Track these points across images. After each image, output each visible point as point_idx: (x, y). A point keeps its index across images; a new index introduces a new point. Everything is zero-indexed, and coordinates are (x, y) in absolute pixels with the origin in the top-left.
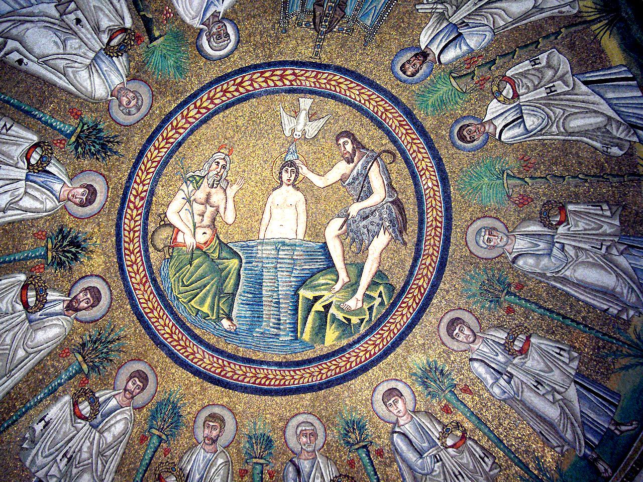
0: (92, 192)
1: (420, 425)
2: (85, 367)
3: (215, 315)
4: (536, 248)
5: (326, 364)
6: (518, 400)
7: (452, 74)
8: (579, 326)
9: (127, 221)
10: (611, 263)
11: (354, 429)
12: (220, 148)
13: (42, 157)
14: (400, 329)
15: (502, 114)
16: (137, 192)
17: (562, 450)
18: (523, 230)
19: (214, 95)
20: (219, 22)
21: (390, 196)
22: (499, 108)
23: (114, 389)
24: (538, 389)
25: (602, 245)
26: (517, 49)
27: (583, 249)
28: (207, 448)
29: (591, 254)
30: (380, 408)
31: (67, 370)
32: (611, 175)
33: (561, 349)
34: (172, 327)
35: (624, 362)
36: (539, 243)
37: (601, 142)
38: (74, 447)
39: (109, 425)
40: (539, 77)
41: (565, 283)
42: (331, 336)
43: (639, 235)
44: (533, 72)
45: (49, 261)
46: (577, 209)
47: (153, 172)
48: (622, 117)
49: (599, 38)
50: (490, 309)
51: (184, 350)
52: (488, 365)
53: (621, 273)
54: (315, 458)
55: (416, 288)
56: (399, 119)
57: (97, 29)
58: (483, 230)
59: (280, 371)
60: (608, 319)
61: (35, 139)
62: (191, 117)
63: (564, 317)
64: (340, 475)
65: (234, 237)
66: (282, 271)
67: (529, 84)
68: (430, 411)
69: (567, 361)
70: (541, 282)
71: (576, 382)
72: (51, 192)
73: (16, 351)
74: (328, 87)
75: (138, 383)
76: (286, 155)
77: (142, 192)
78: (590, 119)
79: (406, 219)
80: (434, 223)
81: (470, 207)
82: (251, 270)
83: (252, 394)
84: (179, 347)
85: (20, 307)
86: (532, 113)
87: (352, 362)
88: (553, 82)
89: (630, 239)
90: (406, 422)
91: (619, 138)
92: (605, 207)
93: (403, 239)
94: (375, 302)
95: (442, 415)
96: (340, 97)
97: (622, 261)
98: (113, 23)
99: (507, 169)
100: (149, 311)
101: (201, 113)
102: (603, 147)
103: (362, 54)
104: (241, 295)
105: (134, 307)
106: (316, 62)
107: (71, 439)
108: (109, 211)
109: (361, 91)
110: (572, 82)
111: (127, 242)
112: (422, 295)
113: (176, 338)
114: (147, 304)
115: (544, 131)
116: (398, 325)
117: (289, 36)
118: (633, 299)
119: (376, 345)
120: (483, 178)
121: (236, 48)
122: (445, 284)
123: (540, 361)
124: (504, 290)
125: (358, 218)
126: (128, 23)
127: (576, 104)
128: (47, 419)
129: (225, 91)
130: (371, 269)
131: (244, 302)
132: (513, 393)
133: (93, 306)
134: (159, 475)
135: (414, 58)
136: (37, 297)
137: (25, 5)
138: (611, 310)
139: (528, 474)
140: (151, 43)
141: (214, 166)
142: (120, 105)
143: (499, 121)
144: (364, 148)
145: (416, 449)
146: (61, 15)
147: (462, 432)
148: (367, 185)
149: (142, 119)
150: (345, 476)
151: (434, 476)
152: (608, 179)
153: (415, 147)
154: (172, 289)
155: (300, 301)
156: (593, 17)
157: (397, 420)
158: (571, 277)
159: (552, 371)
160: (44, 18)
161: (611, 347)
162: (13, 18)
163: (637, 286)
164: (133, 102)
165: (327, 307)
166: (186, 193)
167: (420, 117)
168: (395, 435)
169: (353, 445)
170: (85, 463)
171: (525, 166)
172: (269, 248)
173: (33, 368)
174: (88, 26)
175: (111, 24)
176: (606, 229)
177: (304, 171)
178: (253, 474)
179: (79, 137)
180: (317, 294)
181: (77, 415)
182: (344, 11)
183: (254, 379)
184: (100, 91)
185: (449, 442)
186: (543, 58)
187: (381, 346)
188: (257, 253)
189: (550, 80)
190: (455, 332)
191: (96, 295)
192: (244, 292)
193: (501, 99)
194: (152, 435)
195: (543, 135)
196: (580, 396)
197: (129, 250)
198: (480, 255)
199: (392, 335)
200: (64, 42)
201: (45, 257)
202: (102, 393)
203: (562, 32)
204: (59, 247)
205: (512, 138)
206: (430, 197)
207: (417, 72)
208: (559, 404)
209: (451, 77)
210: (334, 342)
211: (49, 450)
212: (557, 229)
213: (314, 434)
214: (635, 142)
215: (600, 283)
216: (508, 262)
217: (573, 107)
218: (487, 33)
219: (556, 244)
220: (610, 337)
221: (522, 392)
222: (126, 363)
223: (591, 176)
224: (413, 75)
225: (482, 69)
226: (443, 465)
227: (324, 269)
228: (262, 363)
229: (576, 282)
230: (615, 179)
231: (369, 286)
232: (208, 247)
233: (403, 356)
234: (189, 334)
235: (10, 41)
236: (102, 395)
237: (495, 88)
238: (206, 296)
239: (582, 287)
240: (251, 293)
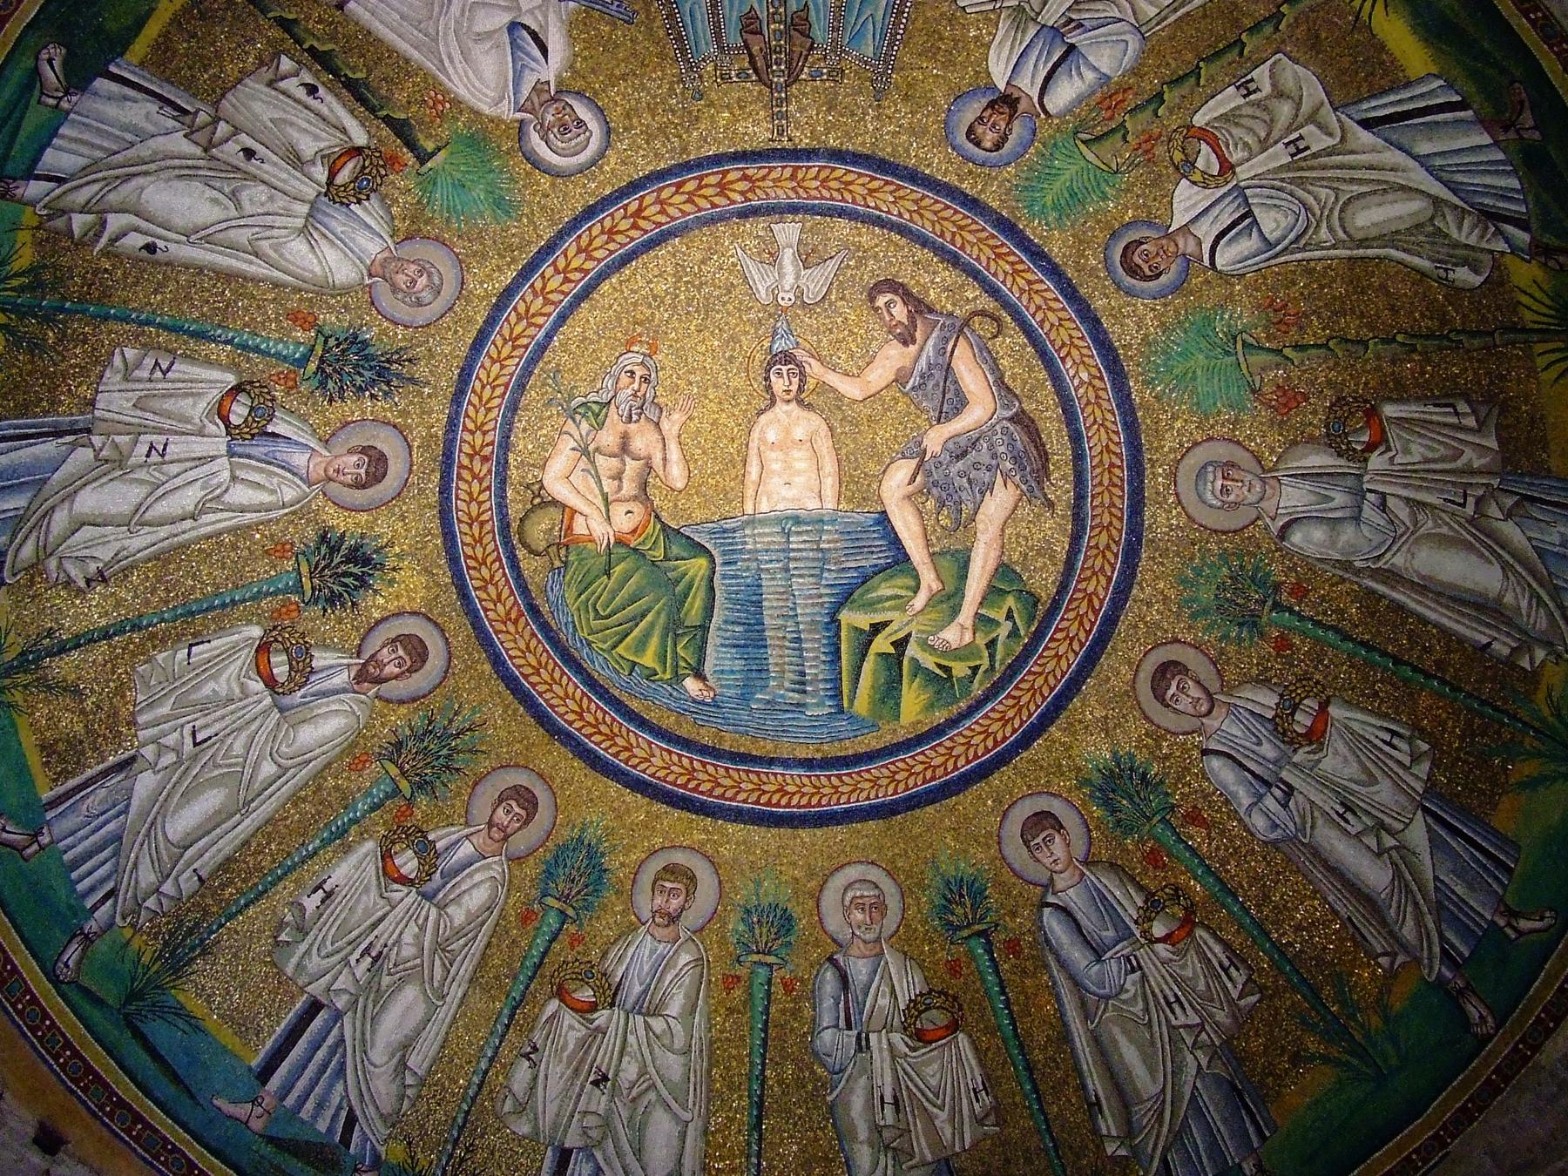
0: (377, 464)
1: (1097, 889)
2: (405, 786)
3: (668, 671)
5: (903, 760)
6: (1303, 844)
7: (1079, 135)
9: (462, 506)
10: (1488, 536)
11: (961, 896)
12: (630, 343)
13: (252, 408)
14: (1055, 686)
15: (1207, 210)
16: (473, 447)
17: (1392, 963)
19: (590, 244)
20: (554, 100)
21: (1007, 407)
23: (467, 824)
24: (1347, 821)
25: (1465, 496)
26: (1201, 64)
28: (659, 932)
30: (1015, 851)
31: (368, 794)
32: (1463, 331)
33: (1394, 733)
34: (581, 700)
35: (1529, 769)
37: (1429, 258)
38: (386, 936)
39: (457, 892)
41: (1393, 583)
42: (913, 704)
43: (1543, 474)
44: (1249, 111)
45: (309, 593)
46: (1404, 415)
47: (500, 405)
50: (1240, 640)
51: (608, 743)
52: (1241, 765)
53: (1511, 561)
54: (882, 953)
55: (1083, 598)
56: (992, 242)
57: (296, 161)
59: (809, 777)
61: (231, 379)
62: (552, 292)
64: (931, 991)
65: (695, 516)
66: (801, 576)
67: (1249, 139)
68: (1119, 862)
69: (1407, 760)
70: (1343, 580)
71: (1426, 810)
72: (290, 471)
73: (257, 766)
74: (825, 193)
75: (517, 810)
76: (773, 342)
77: (482, 447)
78: (1396, 205)
79: (1046, 453)
80: (1105, 455)
81: (1175, 417)
82: (733, 577)
83: (753, 823)
84: (597, 738)
85: (257, 686)
86: (1269, 202)
87: (958, 757)
88: (1296, 130)
90: (1070, 883)
91: (1467, 246)
92: (1463, 407)
93: (1045, 495)
94: (999, 630)
95: (1145, 871)
96: (857, 212)
97: (1510, 530)
98: (327, 143)
100: (531, 671)
101: (571, 281)
103: (878, 118)
104: (719, 629)
105: (497, 661)
106: (783, 149)
107: (374, 926)
108: (419, 489)
109: (897, 194)
110: (1337, 125)
111: (468, 545)
112: (1096, 612)
113: (590, 718)
114: (525, 658)
115: (1303, 242)
116: (1052, 681)
117: (711, 104)
118: (1543, 623)
119: (1007, 721)
121: (608, 144)
122: (1142, 589)
123: (1351, 758)
125: (945, 457)
126: (360, 138)
127: (1358, 174)
128: (327, 887)
129: (611, 233)
130: (986, 562)
131: (727, 642)
133: (411, 671)
134: (560, 987)
135: (989, 111)
136: (290, 665)
137: (115, 147)
138: (1496, 646)
139: (1318, 1013)
140: (422, 164)
141: (625, 379)
142: (395, 289)
143: (1204, 228)
144: (931, 311)
145: (1088, 943)
146: (206, 150)
147: (1185, 909)
148: (952, 388)
149: (450, 309)
150: (940, 993)
151: (1124, 1002)
153: (1038, 300)
154: (574, 626)
155: (843, 634)
157: (1051, 879)
158: (1406, 569)
160: (169, 163)
161: (1498, 733)
162: (100, 175)
164: (422, 281)
165: (901, 644)
166: (577, 437)
168: (1047, 911)
169: (960, 928)
170: (408, 964)
172: (767, 530)
173: (294, 795)
174: (275, 158)
175: (322, 145)
177: (814, 369)
178: (751, 986)
179: (322, 360)
180: (878, 618)
181: (391, 875)
182: (809, 37)
183: (757, 794)
184: (343, 271)
185: (1159, 930)
187: (1017, 723)
188: (745, 543)
189: (1291, 124)
190: (1170, 692)
191: (418, 653)
192: (726, 622)
193: (1197, 177)
194: (547, 909)
195: (1303, 249)
196: (1435, 842)
197: (476, 559)
199: (1039, 699)
200: (234, 196)
201: (298, 588)
202: (440, 833)
204: (323, 569)
206: (1089, 403)
207: (1004, 139)
208: (1390, 857)
210: (920, 717)
211: (332, 944)
212: (1366, 460)
213: (880, 906)
214: (1503, 253)
215: (1468, 585)
217: (1352, 181)
219: (1368, 495)
220: (1496, 709)
221: (1312, 827)
222: (489, 773)
223: (1422, 336)
224: (998, 146)
225: (1140, 116)
226: (1144, 976)
227: (889, 566)
228: (771, 762)
229: (1416, 580)
230: (1476, 342)
231: (984, 598)
232: (641, 539)
233: (1064, 744)
234: (617, 711)
235: (111, 218)
236: (441, 837)
237: (1178, 156)
238: (647, 636)
240: (739, 624)
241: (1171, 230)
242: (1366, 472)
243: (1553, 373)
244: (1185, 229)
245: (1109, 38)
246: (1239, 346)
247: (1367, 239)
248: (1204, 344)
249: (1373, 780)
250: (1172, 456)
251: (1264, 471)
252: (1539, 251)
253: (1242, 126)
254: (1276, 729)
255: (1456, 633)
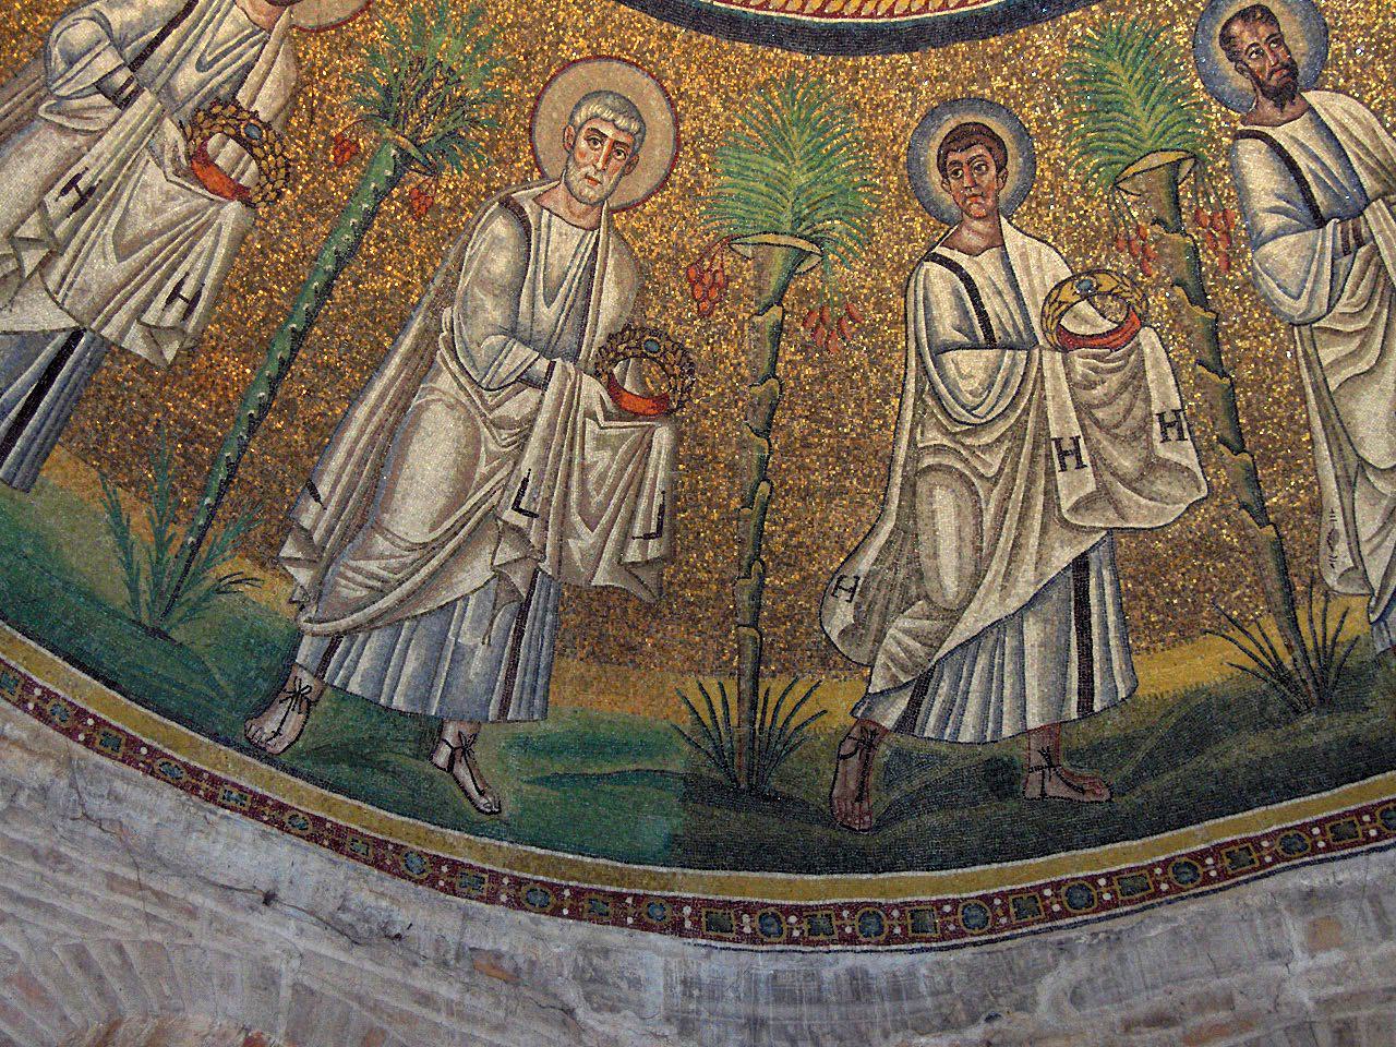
4: (540, 290)
6: (36, 106)
7: (1188, 165)
8: (264, 383)
15: (1015, 286)
18: (611, 262)
22: (1036, 282)
24: (65, 191)
25: (532, 515)
27: (522, 448)
29: (504, 472)
33: (192, 303)
36: (555, 306)
40: (1116, 426)
43: (559, 645)
44: (1138, 412)
46: (654, 454)
48: (957, 656)
49: (1231, 634)
50: (367, 81)
52: (173, 23)
53: (434, 562)
58: (634, 127)
60: (283, 490)
63: (299, 337)
67: (1099, 391)
69: (150, 317)
70: (426, 282)
71: (76, 335)
81: (727, 102)
88: (1094, 464)
89: (546, 610)
92: (654, 549)
97: (474, 575)
99: (823, 255)
102: (857, 578)
110: (1087, 523)
118: (352, 592)
120: (811, 169)
123: (160, 221)
124: (419, 147)
127: (1011, 521)
132: (63, 92)
138: (314, 507)
143: (990, 270)
152: (749, 576)
156: (1304, 627)
158: (432, 390)
159: (121, 258)
163: (389, 610)
167: (1076, 20)
171: (821, 319)
176: (582, 542)
186: (1184, 454)
195: (919, 393)
196: (28, 342)
198: (554, 94)
203: (1261, 525)
205: (926, 298)
207: (1233, 57)
209: (1181, 155)
212: (597, 375)
215: (402, 485)
216: (508, 185)
217: (1002, 512)
218: (1302, 303)
224: (1227, 39)
229: (415, 402)
237: (1107, 283)
239: (397, 422)
241: (1004, 221)
242: (578, 371)
243: (695, 697)
244: (997, 241)
245: (1311, 278)
246: (802, 244)
247: (914, 494)
248: (819, 190)
249: (123, 252)
250: (670, 73)
251: (612, 211)
252: (868, 736)
253: (1119, 393)
254: (218, 101)
255: (334, 443)
